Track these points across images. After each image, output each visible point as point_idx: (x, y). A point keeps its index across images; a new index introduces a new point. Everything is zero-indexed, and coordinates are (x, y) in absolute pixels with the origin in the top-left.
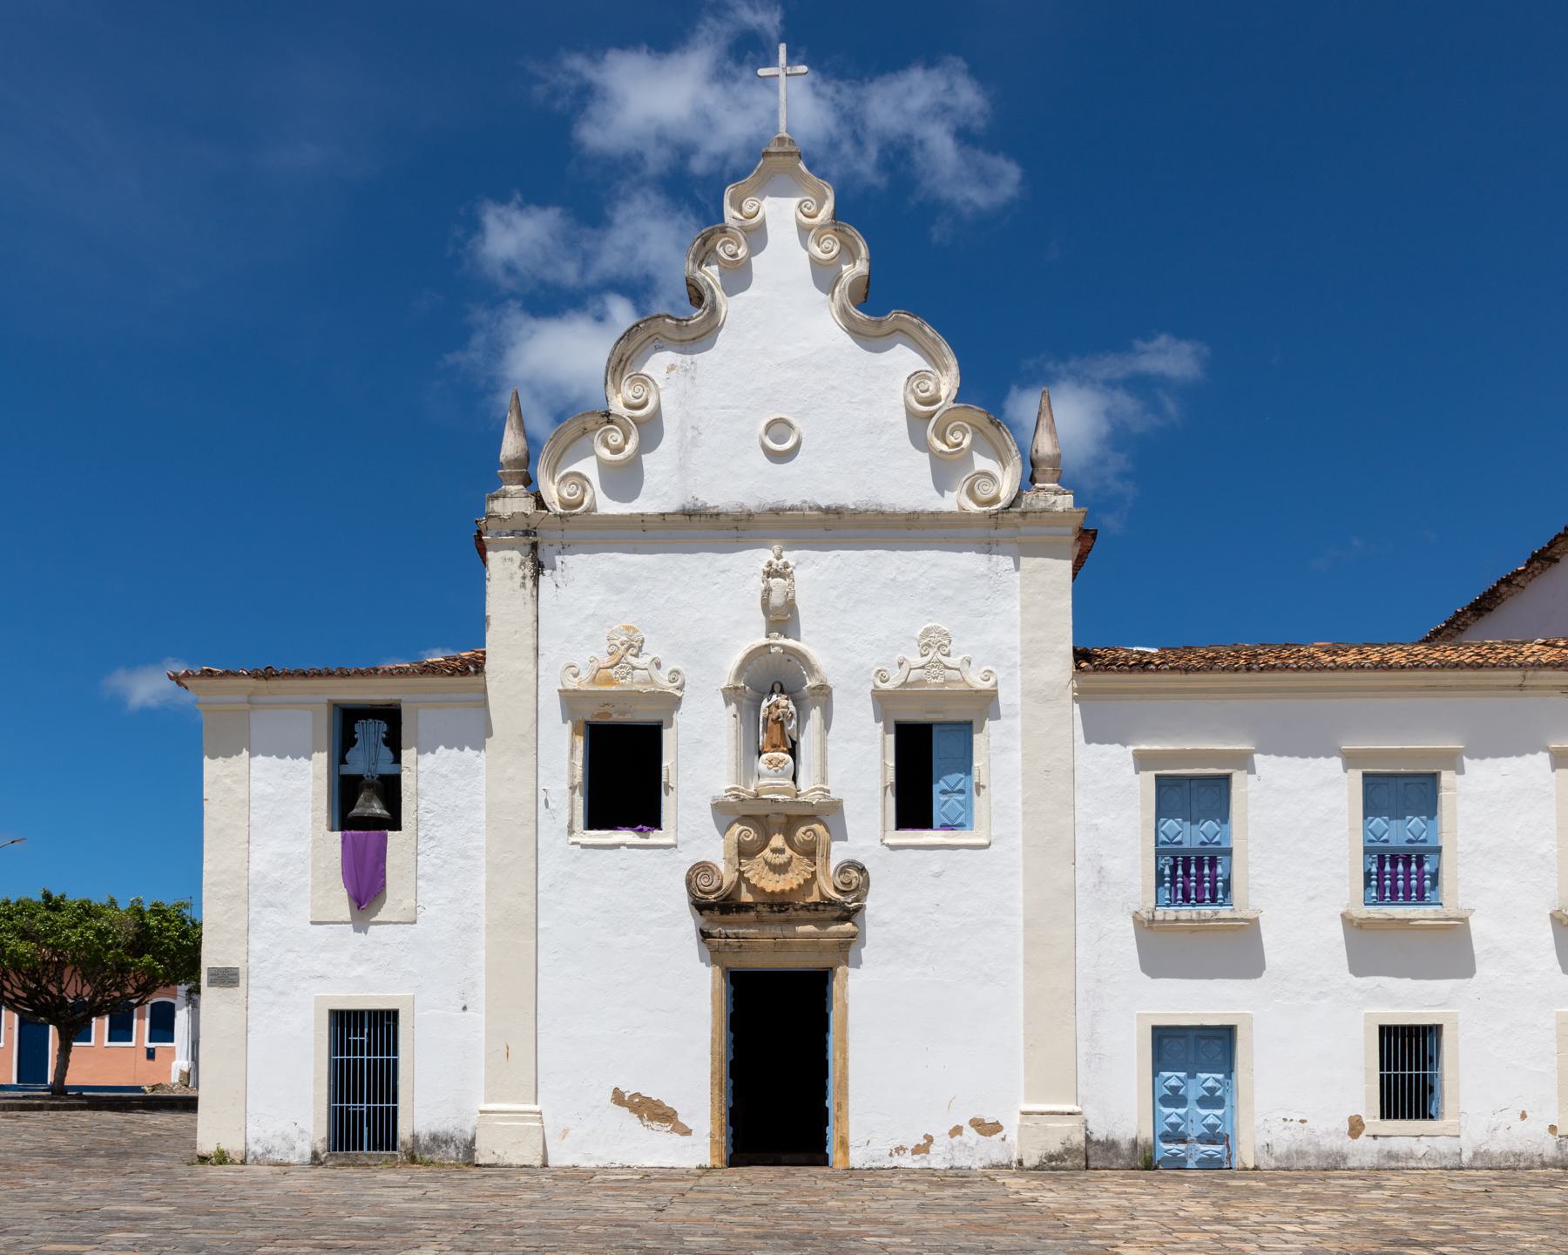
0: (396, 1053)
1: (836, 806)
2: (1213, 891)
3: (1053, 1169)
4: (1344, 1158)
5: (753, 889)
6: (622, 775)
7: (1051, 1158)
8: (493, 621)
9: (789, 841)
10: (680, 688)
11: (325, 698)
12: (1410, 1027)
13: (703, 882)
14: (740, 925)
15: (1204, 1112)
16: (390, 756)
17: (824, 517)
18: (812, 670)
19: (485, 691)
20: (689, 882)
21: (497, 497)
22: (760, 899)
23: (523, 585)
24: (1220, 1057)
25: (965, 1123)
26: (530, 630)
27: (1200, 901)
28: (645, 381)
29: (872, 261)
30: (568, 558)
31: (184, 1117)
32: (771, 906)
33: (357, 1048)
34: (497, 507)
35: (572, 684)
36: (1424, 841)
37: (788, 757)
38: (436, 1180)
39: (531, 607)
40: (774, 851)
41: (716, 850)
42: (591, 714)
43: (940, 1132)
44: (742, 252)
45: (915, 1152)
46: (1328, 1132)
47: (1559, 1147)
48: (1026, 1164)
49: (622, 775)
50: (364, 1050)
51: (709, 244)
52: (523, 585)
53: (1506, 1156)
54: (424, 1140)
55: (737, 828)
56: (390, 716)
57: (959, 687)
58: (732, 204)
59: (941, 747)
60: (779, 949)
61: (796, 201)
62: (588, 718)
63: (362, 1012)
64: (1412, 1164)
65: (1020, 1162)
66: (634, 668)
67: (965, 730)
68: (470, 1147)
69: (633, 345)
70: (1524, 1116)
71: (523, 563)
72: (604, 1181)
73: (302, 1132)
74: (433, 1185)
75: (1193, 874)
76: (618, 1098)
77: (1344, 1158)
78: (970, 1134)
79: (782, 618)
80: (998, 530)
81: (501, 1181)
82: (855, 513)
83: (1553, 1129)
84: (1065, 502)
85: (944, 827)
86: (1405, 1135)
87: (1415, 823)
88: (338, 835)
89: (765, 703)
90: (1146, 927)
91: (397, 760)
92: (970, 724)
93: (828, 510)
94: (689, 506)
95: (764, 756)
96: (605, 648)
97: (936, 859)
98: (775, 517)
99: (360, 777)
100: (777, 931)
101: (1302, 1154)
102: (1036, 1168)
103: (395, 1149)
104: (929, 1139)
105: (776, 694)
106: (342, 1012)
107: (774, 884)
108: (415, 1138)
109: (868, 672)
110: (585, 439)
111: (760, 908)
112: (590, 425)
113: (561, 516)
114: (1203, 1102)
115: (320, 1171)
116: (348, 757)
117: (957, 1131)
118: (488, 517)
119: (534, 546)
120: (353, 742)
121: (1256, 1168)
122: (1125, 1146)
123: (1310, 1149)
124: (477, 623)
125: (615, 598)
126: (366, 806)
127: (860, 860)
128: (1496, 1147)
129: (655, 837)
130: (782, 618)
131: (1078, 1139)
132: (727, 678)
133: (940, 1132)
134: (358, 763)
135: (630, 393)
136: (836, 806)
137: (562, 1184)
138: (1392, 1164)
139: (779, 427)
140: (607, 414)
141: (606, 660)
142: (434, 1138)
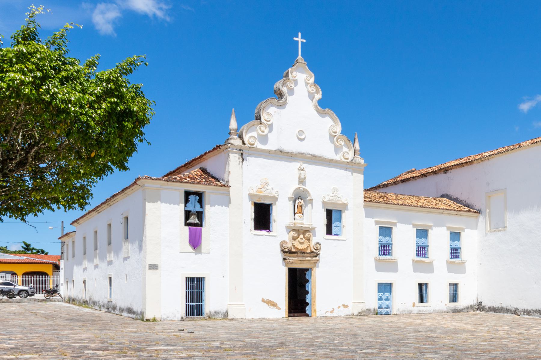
1: (314, 229)
5: (295, 248)
6: (262, 216)
9: (304, 237)
13: (284, 245)
14: (293, 257)
18: (310, 195)
19: (229, 192)
22: (297, 250)
28: (269, 114)
30: (250, 158)
35: (252, 192)
40: (301, 239)
41: (287, 237)
44: (293, 86)
49: (262, 216)
54: (213, 313)
55: (292, 233)
59: (334, 216)
60: (299, 263)
61: (304, 76)
62: (256, 201)
67: (340, 212)
68: (226, 315)
76: (263, 301)
79: (302, 181)
85: (335, 235)
87: (424, 240)
89: (297, 201)
90: (377, 261)
92: (341, 211)
93: (313, 155)
100: (301, 259)
105: (300, 199)
107: (300, 247)
108: (210, 312)
129: (271, 234)
130: (302, 181)
133: (336, 308)
136: (314, 229)
139: (301, 132)
141: (260, 187)
142: (215, 312)
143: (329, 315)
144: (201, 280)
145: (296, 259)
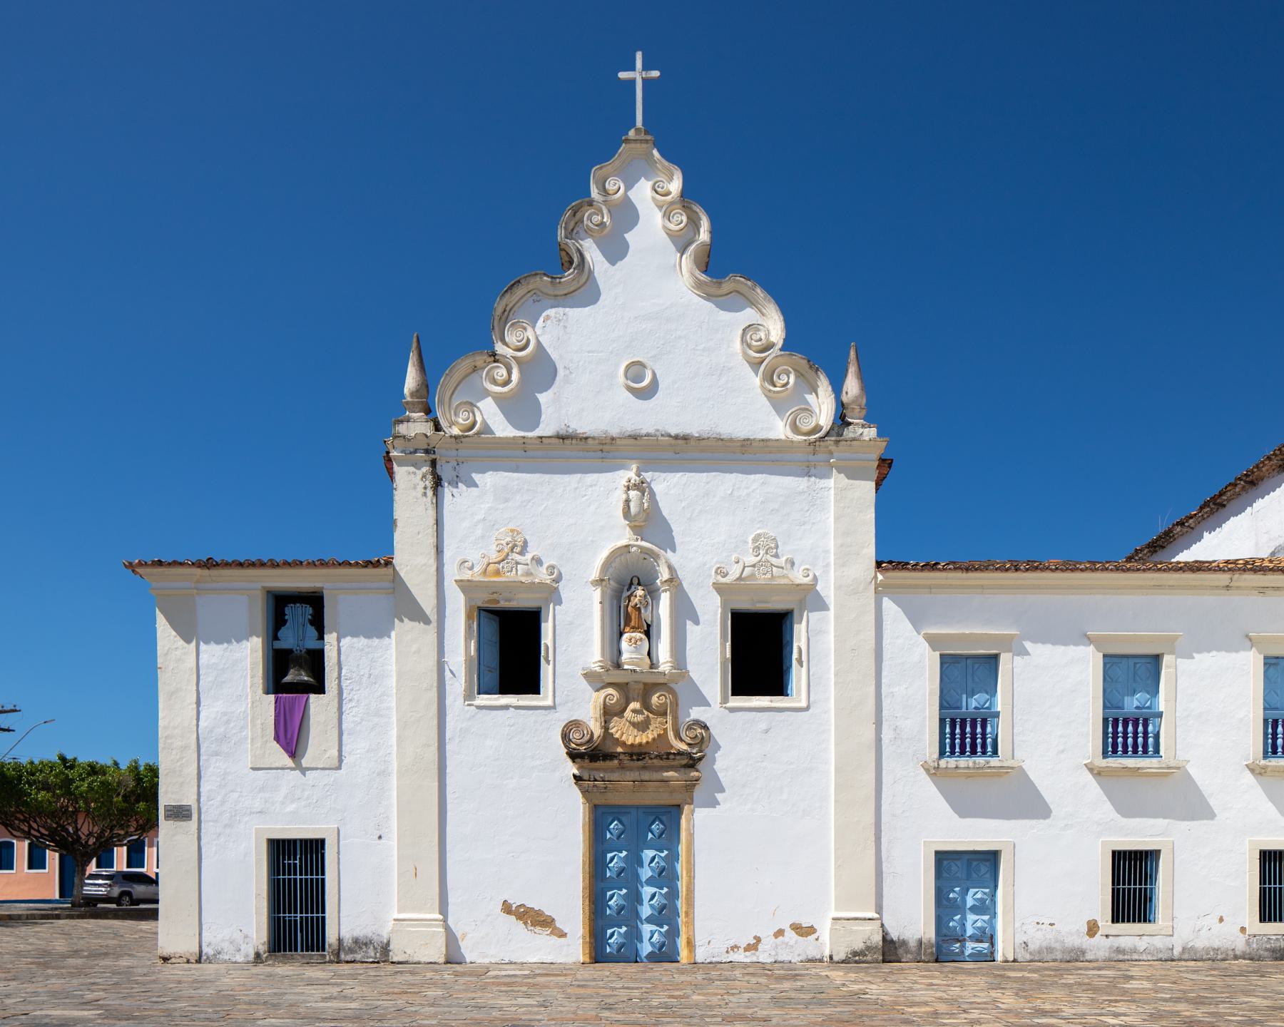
0: (323, 874)
2: (984, 746)
3: (856, 962)
4: (1083, 953)
7: (855, 954)
8: (399, 524)
10: (558, 580)
11: (259, 585)
12: (1136, 852)
14: (605, 770)
15: (976, 917)
16: (315, 634)
17: (673, 442)
20: (565, 737)
21: (402, 422)
23: (425, 494)
24: (988, 875)
25: (786, 927)
26: (431, 530)
27: (974, 752)
29: (712, 232)
31: (145, 925)
32: (631, 755)
33: (292, 870)
34: (402, 429)
35: (467, 575)
36: (1149, 708)
37: (643, 636)
38: (353, 977)
39: (431, 513)
42: (482, 599)
43: (767, 934)
45: (746, 950)
46: (1071, 932)
47: (1248, 943)
48: (836, 958)
50: (297, 872)
51: (578, 215)
52: (425, 494)
53: (1207, 951)
56: (315, 601)
57: (783, 581)
58: (596, 183)
62: (480, 604)
63: (295, 841)
64: (1135, 957)
65: (831, 957)
66: (517, 563)
69: (515, 298)
70: (1221, 920)
71: (424, 476)
72: (496, 977)
73: (246, 937)
74: (351, 982)
75: (966, 732)
77: (1083, 953)
78: (790, 936)
80: (812, 455)
81: (409, 978)
82: (699, 439)
83: (1243, 930)
84: (870, 433)
86: (1131, 935)
88: (272, 697)
91: (321, 638)
93: (676, 437)
94: (563, 432)
95: (625, 636)
96: (494, 547)
97: (763, 720)
98: (632, 441)
99: (291, 651)
100: (635, 775)
101: (1050, 950)
102: (843, 962)
103: (324, 950)
104: (758, 940)
106: (278, 841)
107: (633, 738)
109: (710, 568)
110: (475, 375)
111: (622, 757)
112: (480, 363)
113: (456, 437)
114: (974, 909)
115: (261, 969)
116: (280, 634)
117: (780, 933)
118: (395, 437)
119: (433, 463)
120: (284, 622)
121: (1015, 961)
122: (913, 944)
123: (1057, 946)
124: (391, 524)
125: (501, 506)
126: (295, 673)
127: (702, 719)
128: (1200, 943)
131: (877, 939)
132: (595, 574)
133: (767, 934)
134: (288, 639)
135: (514, 339)
137: (462, 980)
138: (1120, 957)
140: (494, 354)
141: (494, 556)
143: (740, 957)
144: (314, 849)
145: (615, 776)
